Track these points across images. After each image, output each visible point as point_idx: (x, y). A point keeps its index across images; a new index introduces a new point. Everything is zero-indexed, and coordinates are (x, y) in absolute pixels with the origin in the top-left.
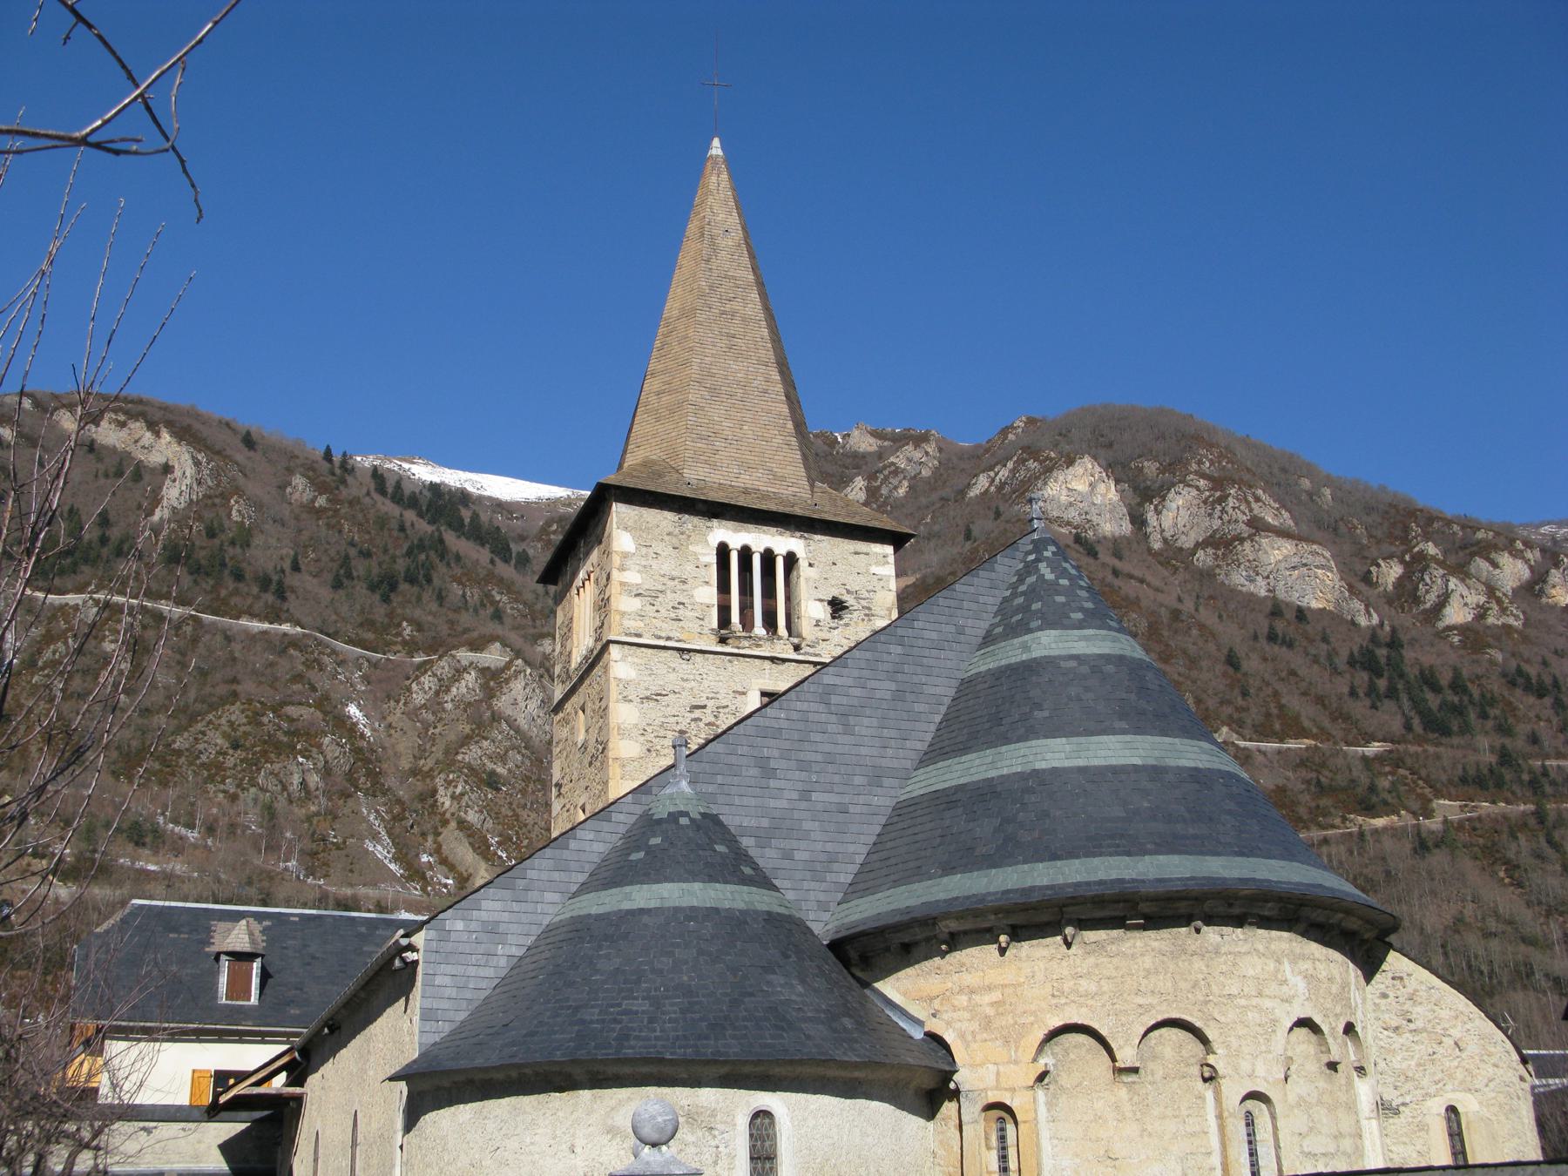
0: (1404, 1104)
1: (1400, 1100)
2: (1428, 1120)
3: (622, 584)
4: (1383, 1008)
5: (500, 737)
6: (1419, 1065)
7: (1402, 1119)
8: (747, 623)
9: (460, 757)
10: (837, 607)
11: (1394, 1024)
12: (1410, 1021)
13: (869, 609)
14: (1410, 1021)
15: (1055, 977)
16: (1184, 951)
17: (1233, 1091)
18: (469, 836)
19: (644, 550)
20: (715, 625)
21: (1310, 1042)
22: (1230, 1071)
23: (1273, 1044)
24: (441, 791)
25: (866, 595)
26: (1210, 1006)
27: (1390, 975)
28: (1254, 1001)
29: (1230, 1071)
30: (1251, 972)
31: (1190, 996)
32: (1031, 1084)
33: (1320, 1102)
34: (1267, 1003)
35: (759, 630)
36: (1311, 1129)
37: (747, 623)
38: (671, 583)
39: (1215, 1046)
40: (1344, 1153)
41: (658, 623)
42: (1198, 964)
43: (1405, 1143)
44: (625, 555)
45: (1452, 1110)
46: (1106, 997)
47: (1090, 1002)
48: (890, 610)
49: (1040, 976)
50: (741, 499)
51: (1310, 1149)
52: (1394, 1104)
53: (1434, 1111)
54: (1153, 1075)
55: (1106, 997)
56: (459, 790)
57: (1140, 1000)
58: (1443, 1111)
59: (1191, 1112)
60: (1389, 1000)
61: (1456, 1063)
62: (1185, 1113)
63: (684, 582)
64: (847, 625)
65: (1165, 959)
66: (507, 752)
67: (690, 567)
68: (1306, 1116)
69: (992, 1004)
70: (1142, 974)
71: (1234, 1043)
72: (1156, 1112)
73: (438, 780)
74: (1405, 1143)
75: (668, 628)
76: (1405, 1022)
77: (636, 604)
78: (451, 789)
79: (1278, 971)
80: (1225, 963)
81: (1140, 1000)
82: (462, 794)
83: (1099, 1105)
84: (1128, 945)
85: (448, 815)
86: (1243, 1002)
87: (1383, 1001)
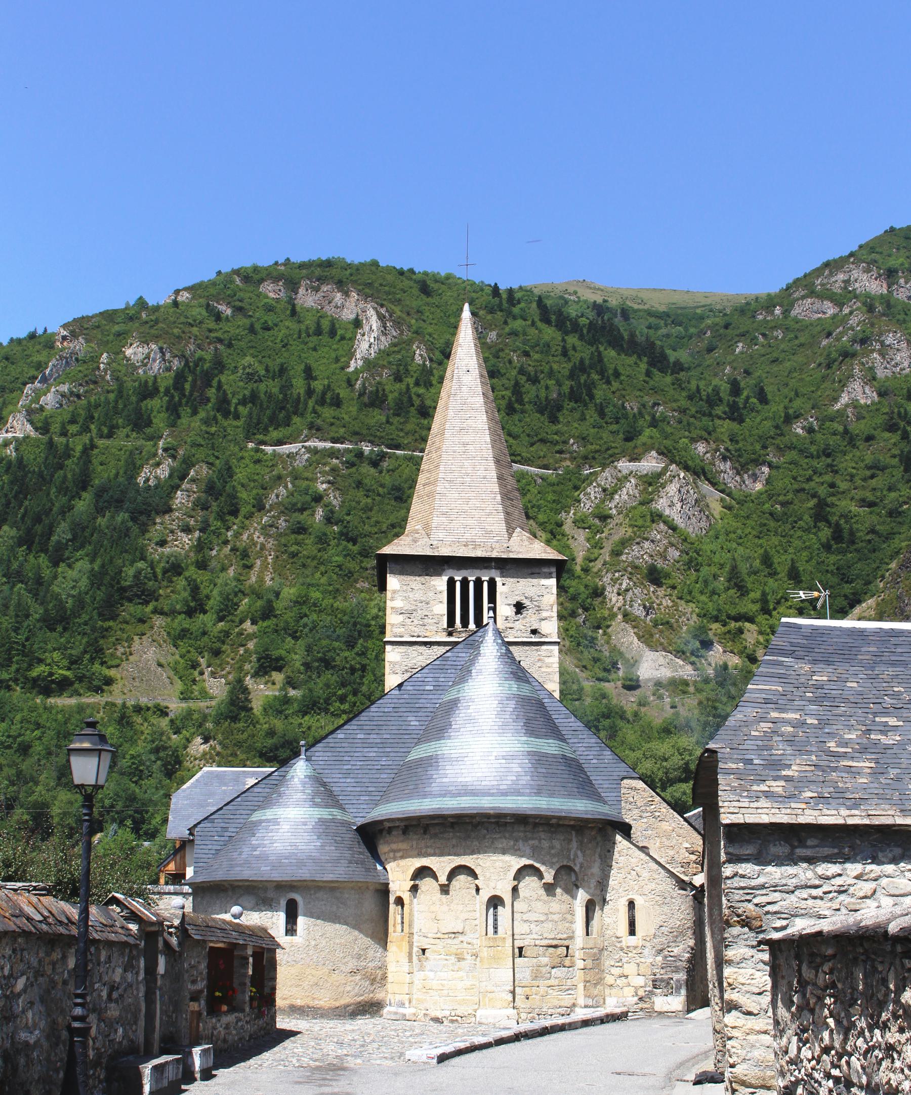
3: (392, 608)
5: (658, 537)
8: (465, 623)
9: (624, 557)
10: (519, 607)
13: (539, 607)
16: (469, 837)
17: (485, 895)
18: (634, 627)
19: (405, 587)
20: (445, 626)
22: (484, 886)
24: (609, 589)
25: (537, 598)
29: (484, 886)
30: (500, 846)
35: (472, 626)
37: (465, 623)
38: (420, 605)
41: (413, 629)
44: (394, 592)
48: (552, 606)
50: (461, 551)
56: (624, 586)
63: (427, 603)
64: (524, 618)
66: (665, 550)
67: (431, 594)
71: (488, 875)
73: (605, 579)
75: (417, 631)
77: (401, 618)
78: (617, 586)
79: (515, 845)
82: (627, 590)
83: (434, 898)
85: (615, 609)
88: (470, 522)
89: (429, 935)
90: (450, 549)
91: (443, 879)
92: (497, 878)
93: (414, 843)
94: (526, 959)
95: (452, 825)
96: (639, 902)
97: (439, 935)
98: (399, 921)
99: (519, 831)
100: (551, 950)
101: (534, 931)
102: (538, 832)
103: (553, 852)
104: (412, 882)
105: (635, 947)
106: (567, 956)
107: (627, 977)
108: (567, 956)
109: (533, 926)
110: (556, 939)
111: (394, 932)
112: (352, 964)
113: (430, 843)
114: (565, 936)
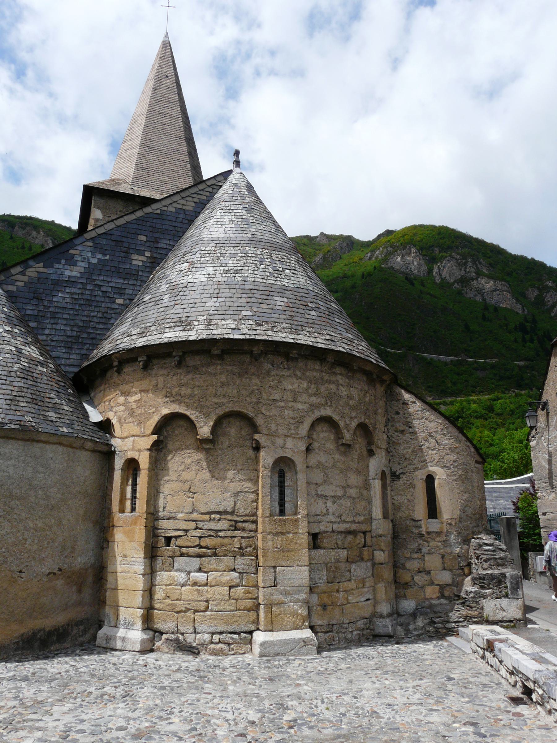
0: (403, 473)
1: (401, 471)
2: (415, 482)
4: (396, 420)
6: (413, 452)
7: (401, 482)
11: (401, 429)
12: (410, 427)
14: (410, 427)
15: (169, 386)
16: (246, 373)
21: (330, 432)
23: (300, 429)
26: (260, 406)
27: (401, 402)
28: (290, 404)
30: (290, 387)
31: (247, 399)
32: (149, 447)
33: (334, 466)
34: (300, 406)
36: (325, 481)
39: (260, 428)
40: (350, 497)
42: (255, 381)
43: (401, 495)
45: (430, 479)
46: (196, 398)
47: (187, 400)
49: (161, 385)
51: (322, 493)
52: (397, 473)
53: (419, 477)
54: (222, 444)
55: (196, 398)
57: (216, 400)
58: (424, 477)
59: (244, 467)
60: (400, 416)
61: (435, 452)
62: (240, 467)
65: (234, 377)
68: (322, 474)
69: (135, 401)
70: (219, 384)
72: (221, 466)
74: (401, 495)
76: (407, 428)
79: (308, 388)
80: (273, 381)
81: (216, 400)
83: (188, 461)
84: (212, 368)
86: (283, 404)
87: (396, 416)
88: (165, 178)
89: (180, 516)
90: (149, 194)
91: (205, 431)
92: (285, 432)
93: (161, 379)
94: (322, 551)
95: (221, 357)
96: (440, 474)
97: (195, 516)
98: (129, 495)
99: (313, 370)
100: (350, 538)
101: (331, 510)
102: (335, 374)
103: (351, 403)
104: (155, 437)
105: (439, 533)
106: (364, 546)
107: (429, 572)
108: (364, 546)
109: (329, 504)
110: (354, 522)
111: (122, 511)
112: (51, 565)
113: (185, 379)
114: (362, 518)
